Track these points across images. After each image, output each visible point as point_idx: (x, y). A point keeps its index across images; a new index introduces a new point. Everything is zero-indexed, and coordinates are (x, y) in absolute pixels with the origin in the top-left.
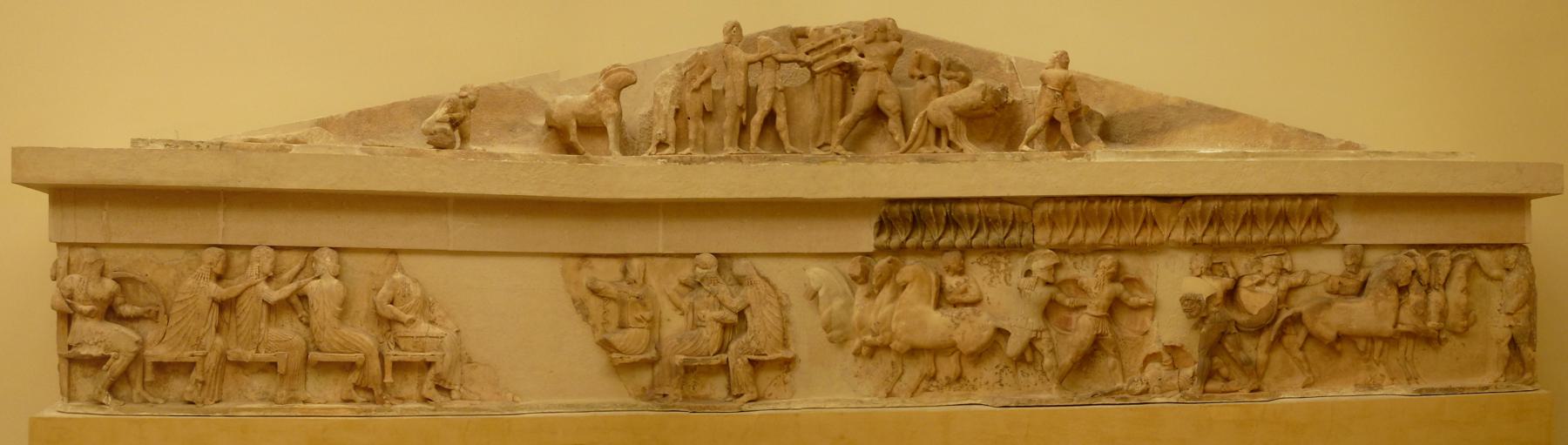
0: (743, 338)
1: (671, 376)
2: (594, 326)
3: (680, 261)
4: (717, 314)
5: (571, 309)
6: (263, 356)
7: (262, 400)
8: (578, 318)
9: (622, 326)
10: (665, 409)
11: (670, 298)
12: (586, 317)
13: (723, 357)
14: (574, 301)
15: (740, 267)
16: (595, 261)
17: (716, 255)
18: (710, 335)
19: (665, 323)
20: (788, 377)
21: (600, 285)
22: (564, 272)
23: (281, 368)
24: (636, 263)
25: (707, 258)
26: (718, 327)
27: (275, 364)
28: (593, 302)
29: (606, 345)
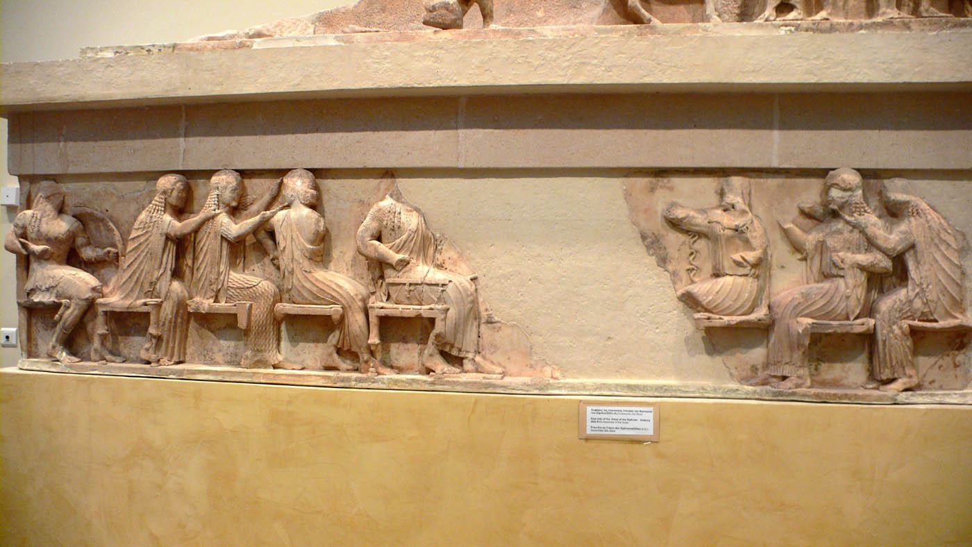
0: (902, 294)
1: (791, 349)
2: (674, 274)
3: (801, 181)
4: (864, 258)
5: (639, 250)
6: (223, 305)
7: (229, 363)
8: (653, 260)
9: (717, 275)
10: (778, 396)
11: (786, 233)
12: (663, 261)
13: (872, 322)
14: (644, 237)
15: (897, 191)
16: (677, 181)
17: (860, 171)
18: (851, 289)
19: (776, 271)
20: (960, 358)
21: (680, 213)
22: (628, 195)
23: (242, 323)
24: (736, 181)
25: (853, 178)
26: (863, 278)
27: (235, 315)
28: (674, 239)
29: (690, 301)
